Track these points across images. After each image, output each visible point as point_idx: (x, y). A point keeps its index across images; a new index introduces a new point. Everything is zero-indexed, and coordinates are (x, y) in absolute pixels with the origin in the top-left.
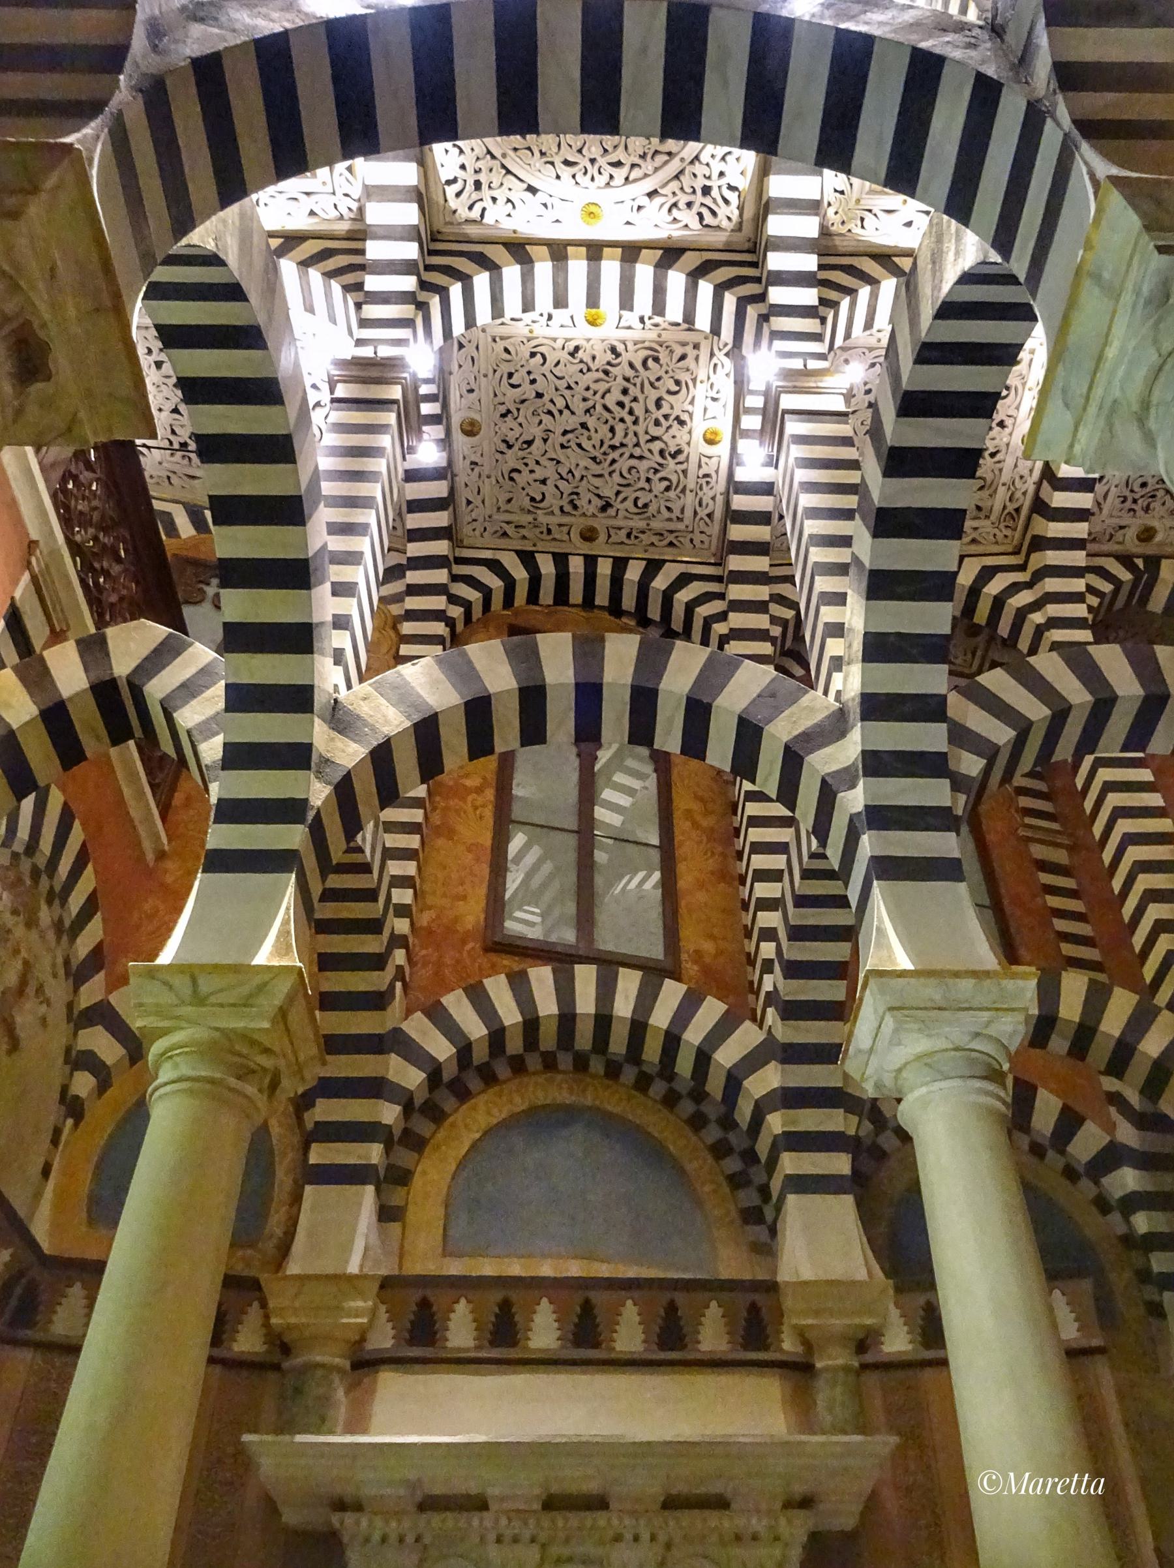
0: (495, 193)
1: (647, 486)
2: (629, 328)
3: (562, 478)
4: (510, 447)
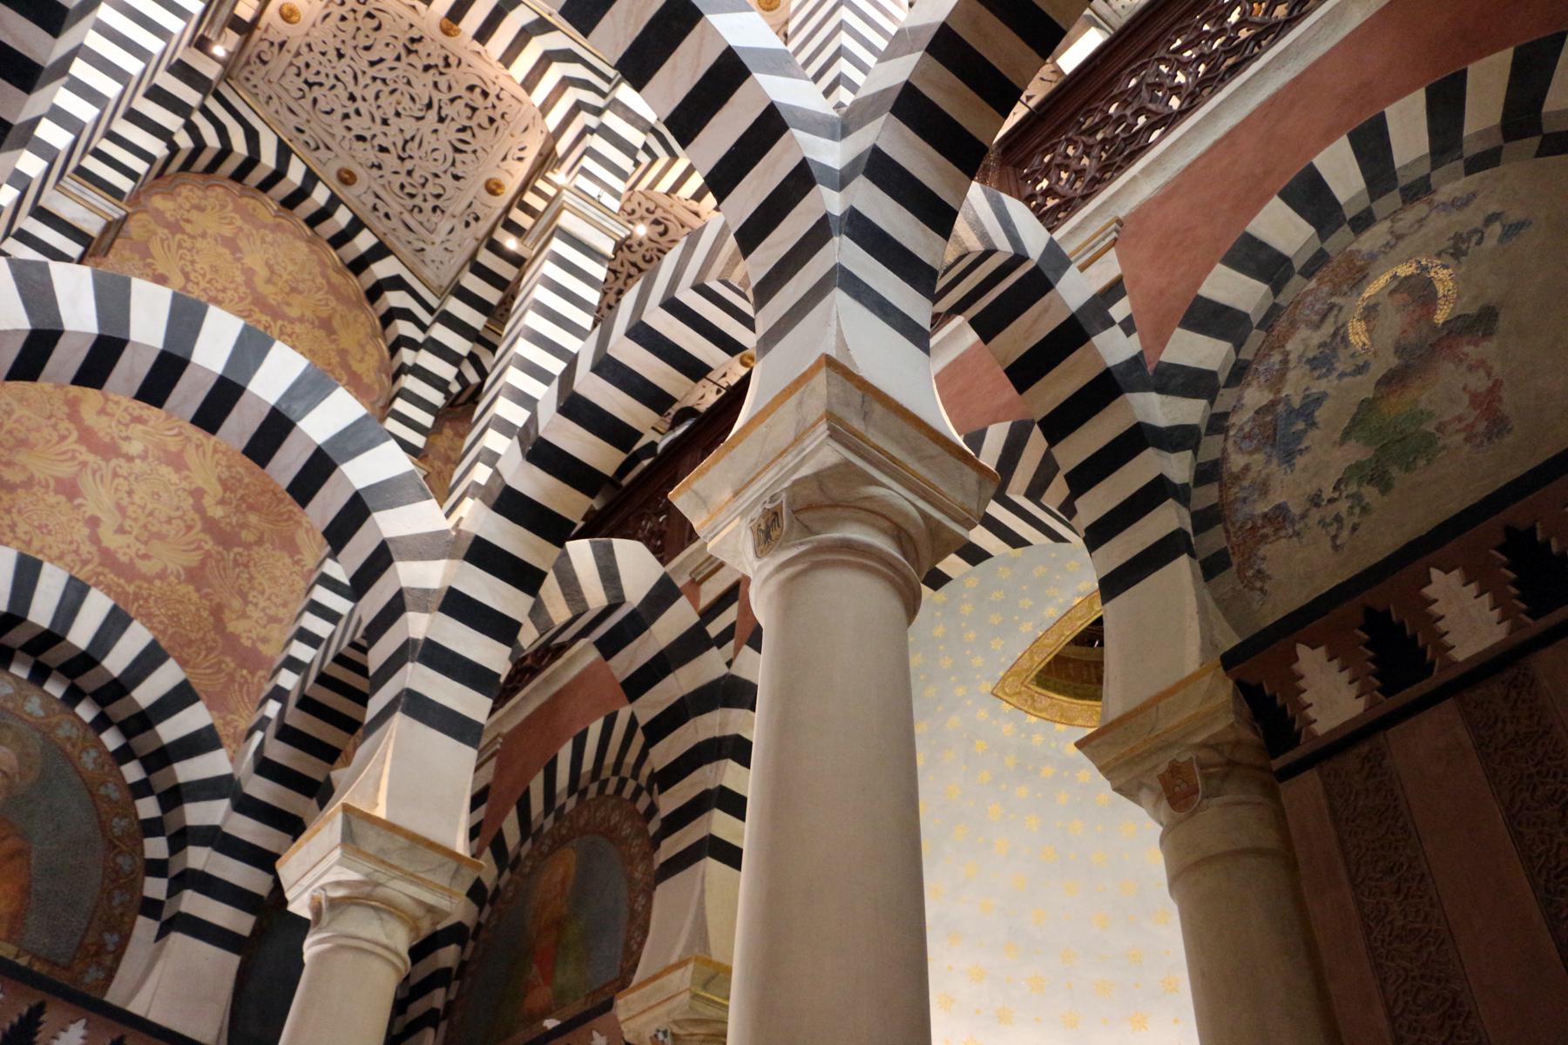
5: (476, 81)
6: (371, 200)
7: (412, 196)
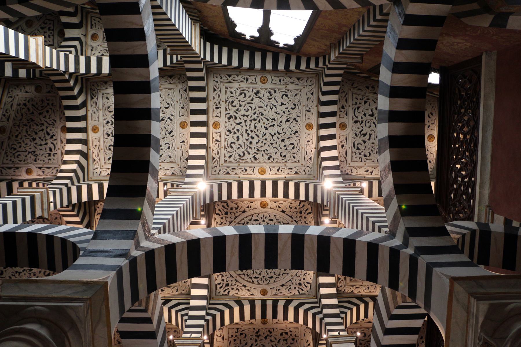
0: (296, 210)
1: (241, 103)
2: (250, 167)
3: (275, 106)
4: (295, 119)
5: (282, 331)
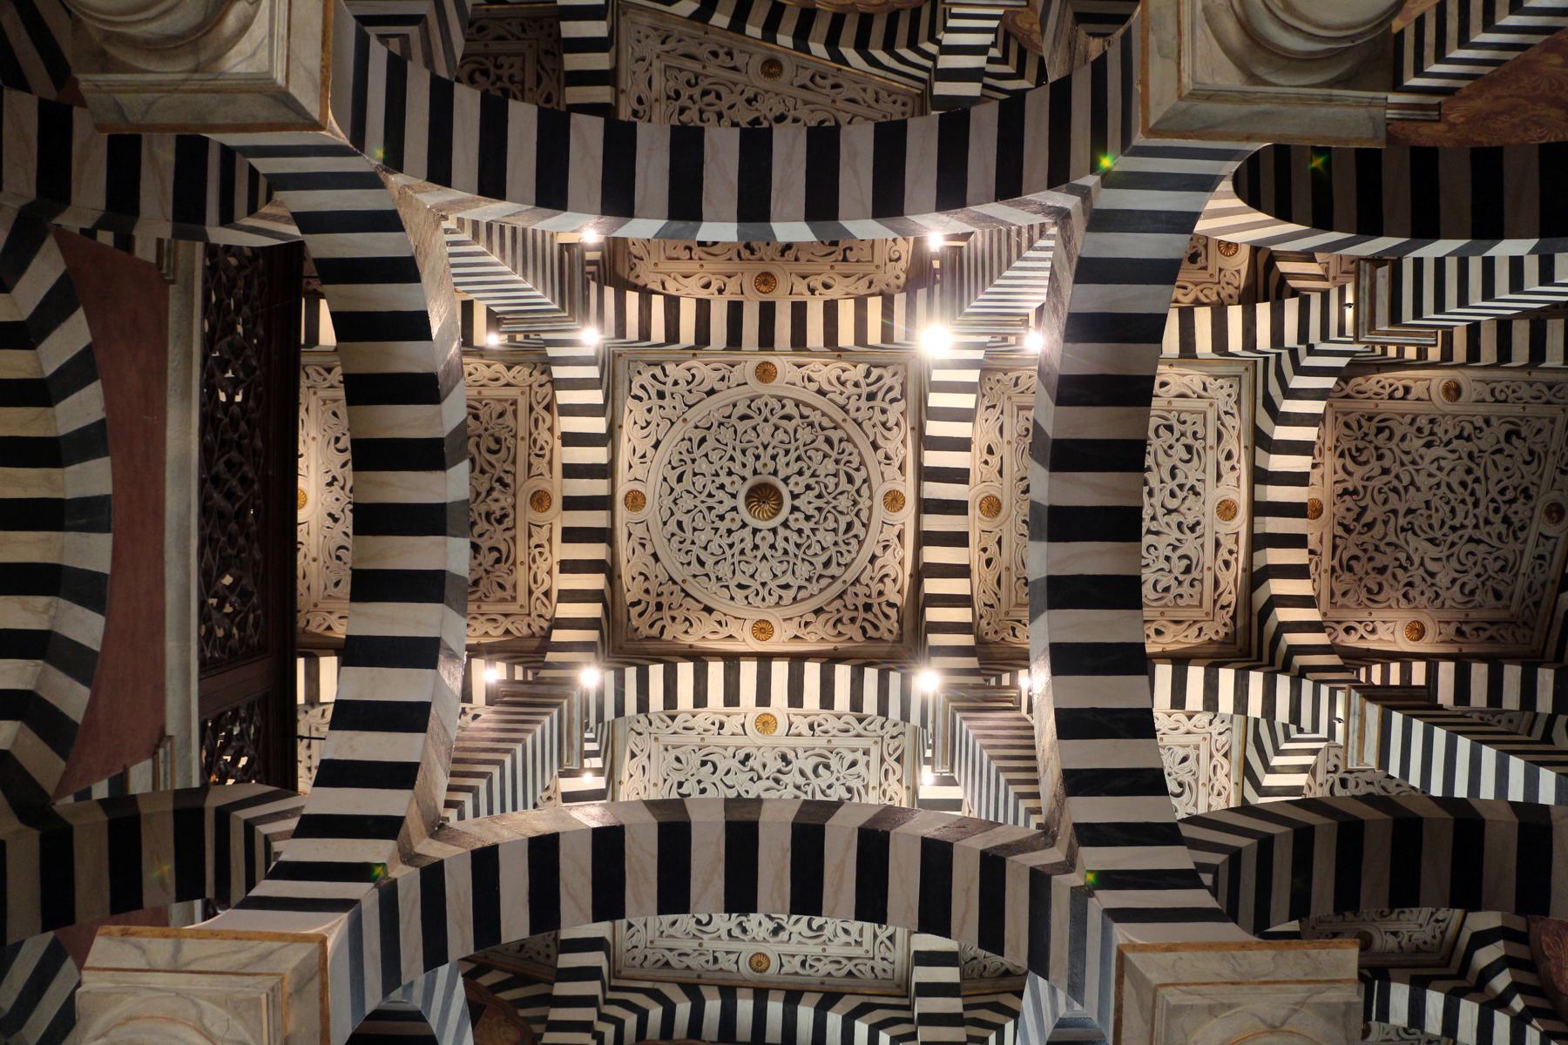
0: (674, 613)
2: (799, 735)
6: (739, 60)
7: (705, 93)
